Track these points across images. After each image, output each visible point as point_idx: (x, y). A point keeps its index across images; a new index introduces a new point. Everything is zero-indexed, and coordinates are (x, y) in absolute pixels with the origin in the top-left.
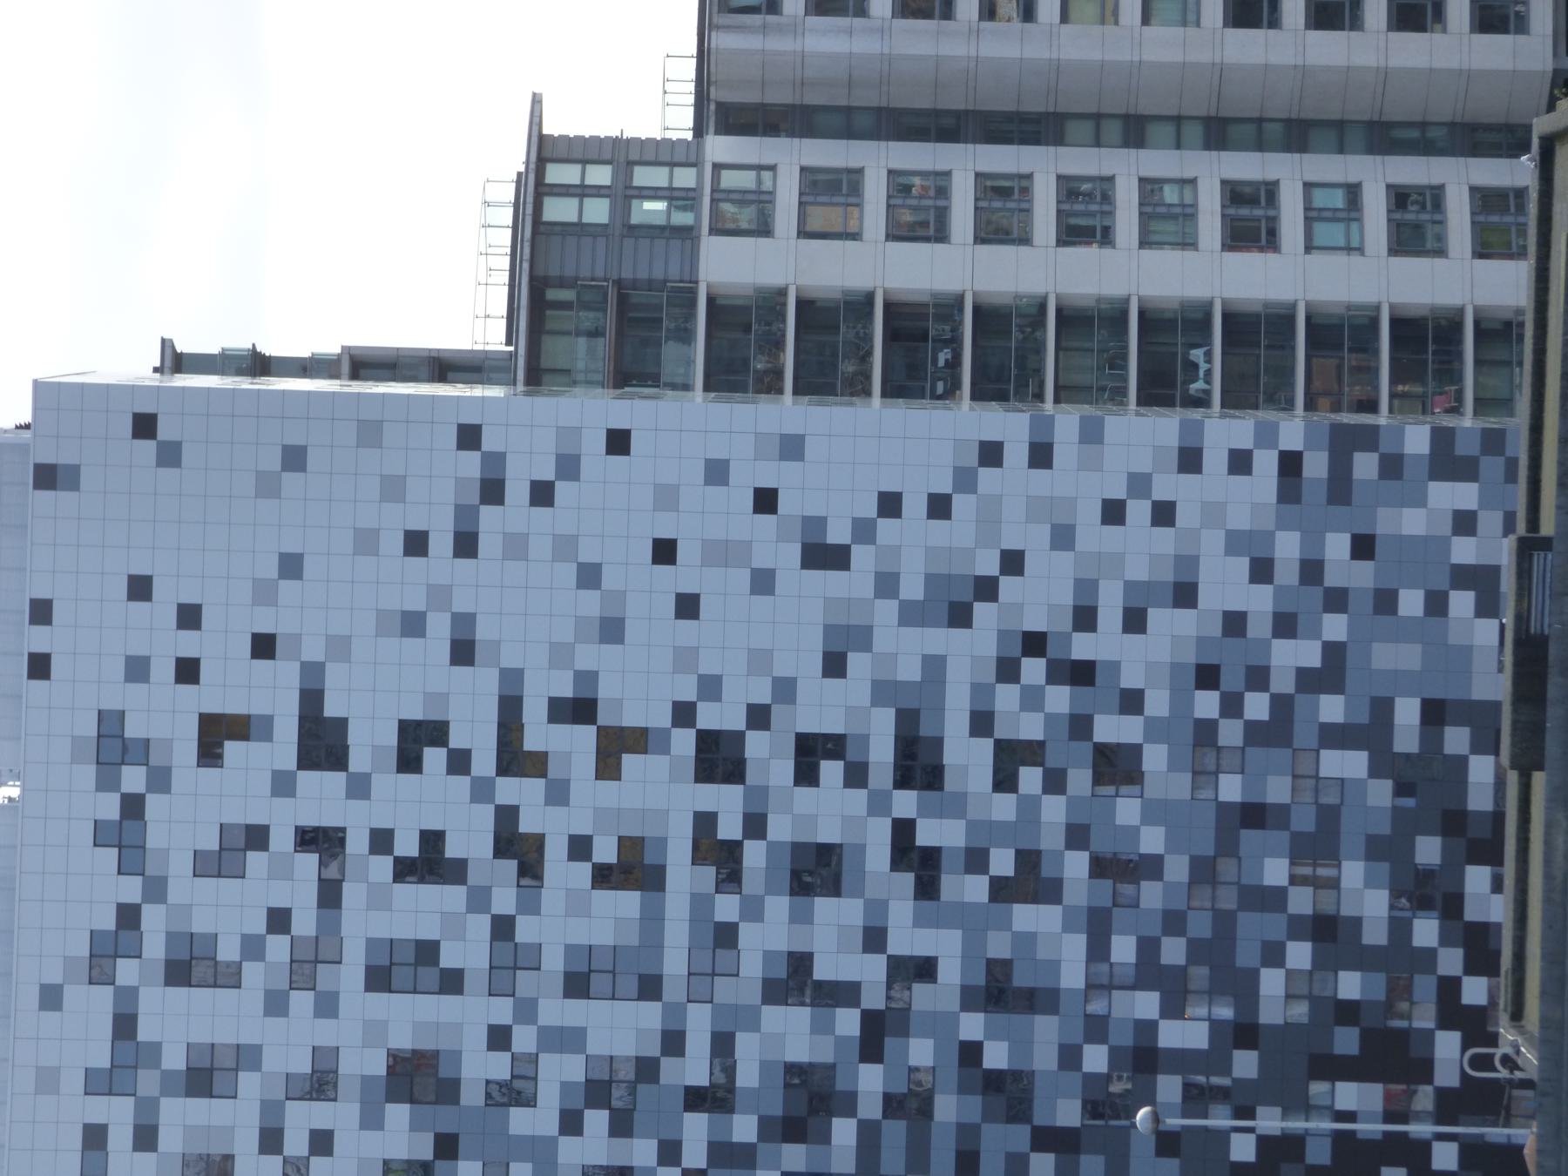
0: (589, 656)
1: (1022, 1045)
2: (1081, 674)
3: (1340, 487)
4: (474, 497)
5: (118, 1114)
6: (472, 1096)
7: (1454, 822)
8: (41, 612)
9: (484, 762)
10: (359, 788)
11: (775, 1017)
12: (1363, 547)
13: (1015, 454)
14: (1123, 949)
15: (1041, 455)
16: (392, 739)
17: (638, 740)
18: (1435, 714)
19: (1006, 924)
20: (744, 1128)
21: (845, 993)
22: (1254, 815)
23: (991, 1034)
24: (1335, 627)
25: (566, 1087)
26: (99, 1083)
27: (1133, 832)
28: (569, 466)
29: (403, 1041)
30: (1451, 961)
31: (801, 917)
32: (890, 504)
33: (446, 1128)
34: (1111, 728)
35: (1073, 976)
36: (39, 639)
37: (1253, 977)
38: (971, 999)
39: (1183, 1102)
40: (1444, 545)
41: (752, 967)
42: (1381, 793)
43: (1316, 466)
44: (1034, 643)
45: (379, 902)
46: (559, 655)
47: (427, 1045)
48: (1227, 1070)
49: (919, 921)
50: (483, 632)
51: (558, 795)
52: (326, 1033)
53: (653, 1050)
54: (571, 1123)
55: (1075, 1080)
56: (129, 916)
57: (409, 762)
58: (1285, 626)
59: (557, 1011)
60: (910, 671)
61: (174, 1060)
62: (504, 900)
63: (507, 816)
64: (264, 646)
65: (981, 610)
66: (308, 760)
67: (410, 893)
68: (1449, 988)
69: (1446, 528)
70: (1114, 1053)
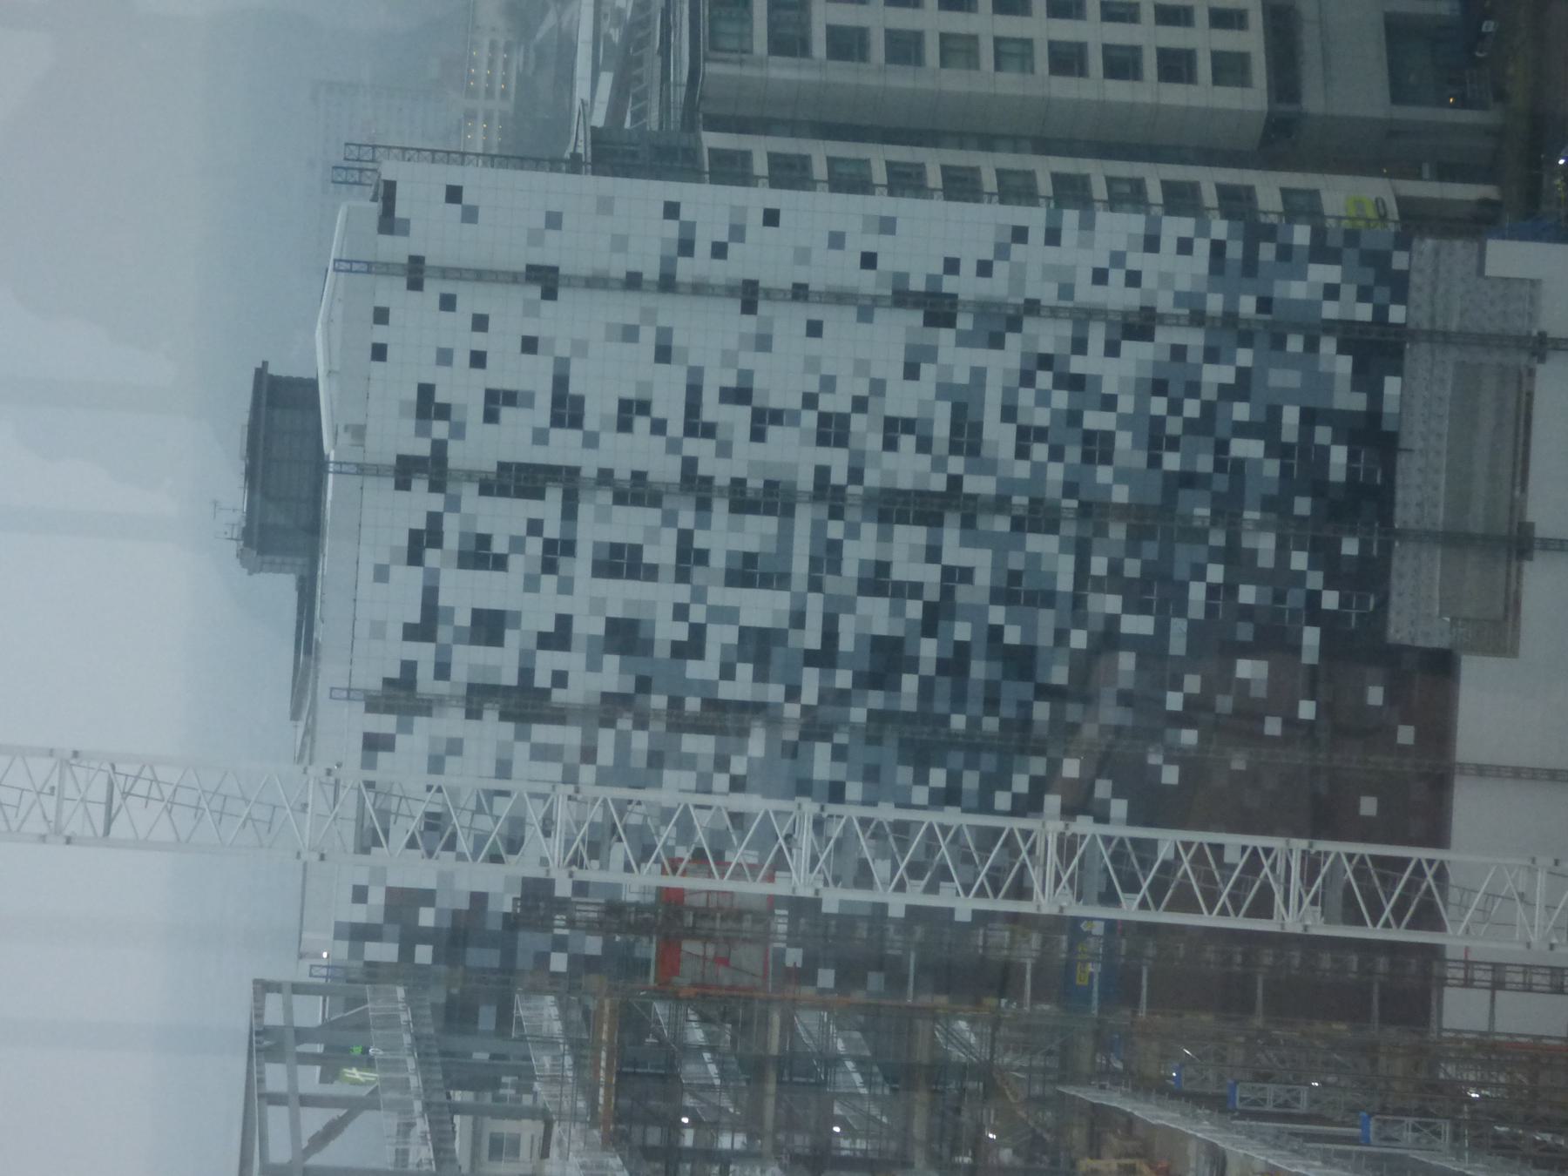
0: (748, 360)
1: (1030, 629)
2: (1076, 383)
3: (1250, 265)
4: (674, 250)
5: (424, 654)
6: (662, 651)
7: (1318, 487)
8: (381, 316)
9: (676, 427)
10: (591, 441)
11: (867, 605)
12: (1265, 304)
13: (1037, 235)
14: (1099, 566)
15: (1053, 237)
16: (613, 408)
17: (777, 417)
18: (1309, 418)
19: (1021, 546)
20: (843, 679)
21: (916, 590)
22: (1188, 479)
23: (1010, 619)
24: (1245, 357)
26: (413, 633)
27: (1107, 489)
28: (738, 233)
29: (617, 612)
30: (1315, 580)
31: (885, 537)
32: (952, 266)
34: (1095, 420)
35: (1065, 583)
36: (380, 334)
37: (1184, 587)
38: (997, 596)
40: (1318, 306)
41: (850, 569)
42: (1272, 468)
43: (1235, 251)
44: (1045, 362)
45: (603, 517)
46: (728, 358)
49: (964, 543)
50: (678, 340)
51: (724, 450)
52: (564, 605)
53: (785, 624)
54: (727, 672)
56: (435, 520)
57: (625, 426)
58: (1212, 355)
59: (720, 595)
60: (962, 377)
61: (464, 619)
62: (687, 519)
63: (690, 464)
64: (530, 345)
65: (1012, 339)
66: (557, 421)
67: (623, 513)
68: (1314, 598)
69: (1319, 294)
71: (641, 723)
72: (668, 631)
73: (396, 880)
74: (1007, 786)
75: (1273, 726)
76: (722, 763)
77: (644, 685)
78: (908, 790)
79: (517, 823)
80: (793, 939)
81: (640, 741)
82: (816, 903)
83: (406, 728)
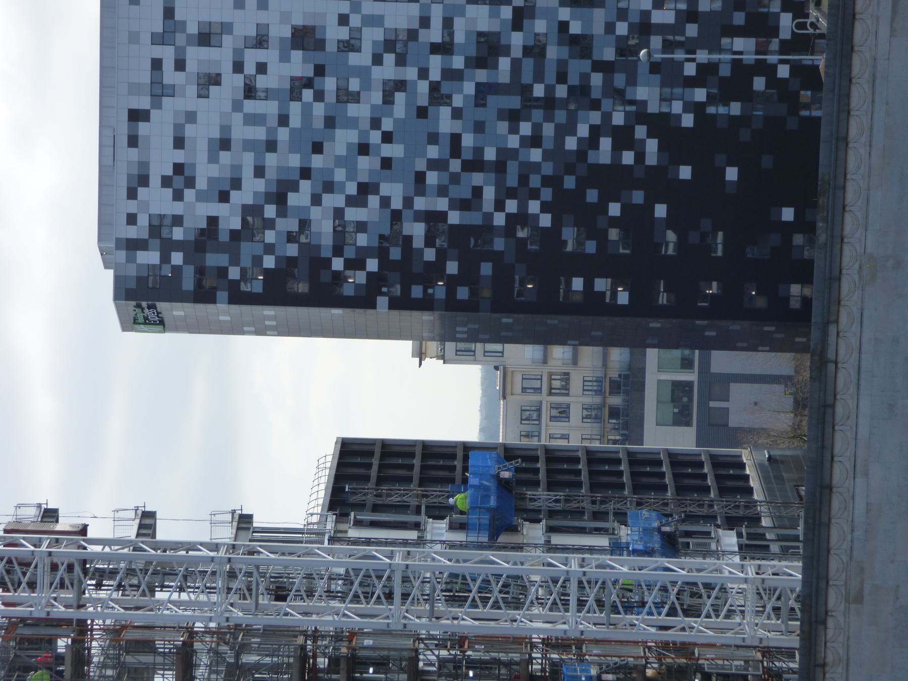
1: (588, 23)
5: (167, 54)
6: (331, 47)
20: (458, 62)
23: (573, 17)
25: (375, 43)
26: (159, 39)
33: (320, 62)
39: (663, 48)
47: (310, 23)
48: (683, 33)
52: (263, 17)
53: (416, 25)
54: (377, 60)
55: (612, 39)
61: (192, 29)
70: (631, 27)
71: (319, 96)
72: (335, 34)
73: (155, 210)
74: (574, 133)
75: (759, 83)
76: (375, 123)
77: (320, 71)
78: (505, 139)
79: (236, 168)
80: (429, 241)
81: (319, 110)
82: (442, 216)
83: (157, 104)
